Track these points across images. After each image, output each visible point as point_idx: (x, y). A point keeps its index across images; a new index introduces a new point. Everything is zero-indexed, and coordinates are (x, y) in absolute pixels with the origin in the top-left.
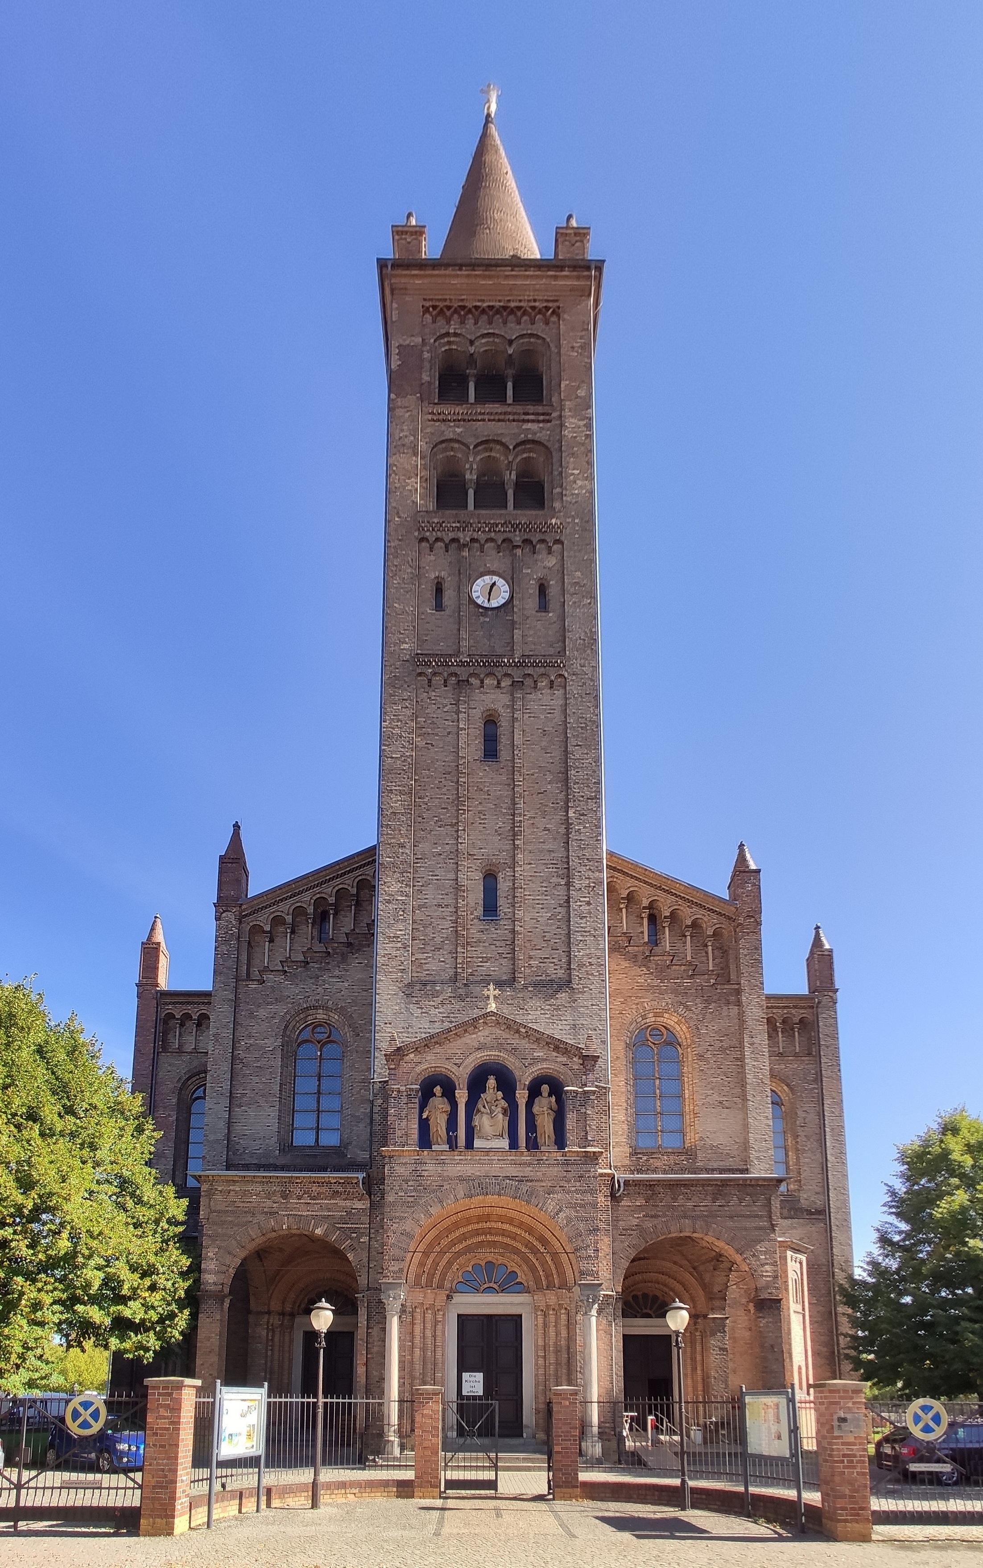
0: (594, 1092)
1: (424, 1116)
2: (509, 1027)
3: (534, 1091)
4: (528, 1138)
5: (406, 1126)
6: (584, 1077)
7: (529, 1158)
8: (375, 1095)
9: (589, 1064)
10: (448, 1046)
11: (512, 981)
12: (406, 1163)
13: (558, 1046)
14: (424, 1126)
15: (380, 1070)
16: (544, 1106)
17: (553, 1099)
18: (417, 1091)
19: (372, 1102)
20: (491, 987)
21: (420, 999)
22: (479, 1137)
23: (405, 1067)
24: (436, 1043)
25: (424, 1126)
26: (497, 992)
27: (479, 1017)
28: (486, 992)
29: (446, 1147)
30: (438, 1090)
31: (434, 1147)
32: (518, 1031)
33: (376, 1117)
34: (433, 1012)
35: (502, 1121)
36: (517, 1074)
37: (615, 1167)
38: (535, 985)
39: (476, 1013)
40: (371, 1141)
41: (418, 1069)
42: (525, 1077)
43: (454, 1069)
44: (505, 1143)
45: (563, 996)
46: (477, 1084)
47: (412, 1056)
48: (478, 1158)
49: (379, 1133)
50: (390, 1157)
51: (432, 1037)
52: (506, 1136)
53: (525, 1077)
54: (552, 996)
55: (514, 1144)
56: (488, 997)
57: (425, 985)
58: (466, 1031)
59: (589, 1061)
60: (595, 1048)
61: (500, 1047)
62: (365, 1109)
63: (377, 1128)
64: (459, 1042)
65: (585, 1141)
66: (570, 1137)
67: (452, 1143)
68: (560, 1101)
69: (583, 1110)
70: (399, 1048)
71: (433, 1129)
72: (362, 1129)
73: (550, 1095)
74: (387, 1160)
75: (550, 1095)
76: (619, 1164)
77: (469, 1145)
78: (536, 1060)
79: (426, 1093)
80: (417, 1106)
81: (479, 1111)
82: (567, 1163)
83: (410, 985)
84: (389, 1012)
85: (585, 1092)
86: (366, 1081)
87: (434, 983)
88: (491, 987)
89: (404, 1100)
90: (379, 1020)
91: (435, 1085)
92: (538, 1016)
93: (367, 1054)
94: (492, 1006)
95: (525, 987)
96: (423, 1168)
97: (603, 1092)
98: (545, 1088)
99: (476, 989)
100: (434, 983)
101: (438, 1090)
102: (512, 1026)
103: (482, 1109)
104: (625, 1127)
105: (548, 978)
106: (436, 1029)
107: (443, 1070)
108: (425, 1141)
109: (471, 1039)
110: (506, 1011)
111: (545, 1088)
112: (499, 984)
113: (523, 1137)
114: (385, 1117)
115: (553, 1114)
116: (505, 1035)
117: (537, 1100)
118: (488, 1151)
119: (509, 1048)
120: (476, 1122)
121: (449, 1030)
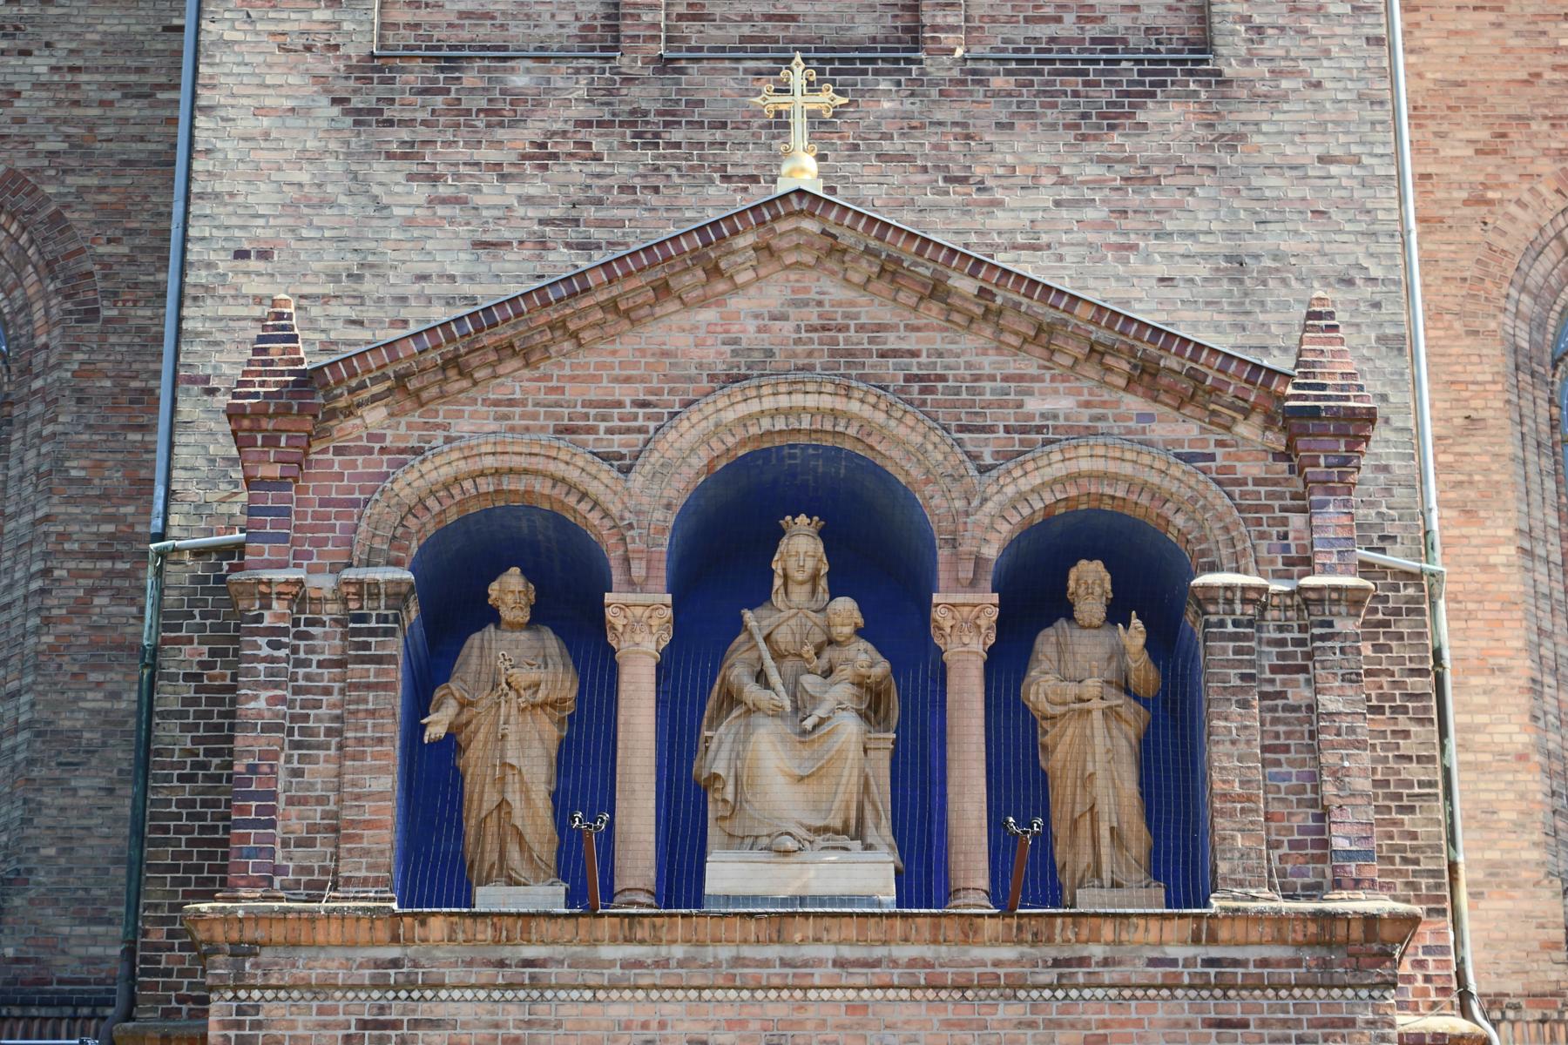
0: (1353, 600)
1: (437, 726)
2: (891, 271)
3: (1031, 595)
4: (1000, 846)
5: (333, 783)
6: (1297, 520)
7: (1008, 953)
8: (169, 620)
9: (1322, 452)
10: (564, 364)
11: (907, 43)
12: (323, 987)
13: (1153, 364)
14: (433, 779)
15: (202, 482)
16: (1085, 671)
17: (1135, 635)
18: (398, 596)
19: (152, 659)
20: (798, 75)
21: (423, 133)
22: (734, 840)
23: (335, 471)
24: (507, 350)
25: (433, 779)
26: (826, 99)
27: (729, 225)
28: (767, 101)
29: (550, 895)
30: (510, 590)
31: (488, 897)
32: (937, 291)
33: (173, 737)
34: (492, 194)
35: (855, 751)
36: (938, 503)
37: (1494, 1001)
38: (1025, 62)
39: (718, 200)
40: (137, 869)
41: (408, 483)
42: (977, 521)
43: (601, 483)
44: (872, 873)
45: (1171, 120)
46: (722, 556)
47: (375, 416)
48: (725, 952)
49: (188, 822)
50: (241, 951)
51: (484, 319)
52: (881, 831)
53: (977, 521)
54: (1112, 118)
55: (924, 880)
56: (781, 123)
57: (451, 62)
58: (663, 290)
59: (1319, 433)
60: (1352, 366)
61: (845, 368)
62: (103, 698)
63: (171, 793)
64: (630, 344)
65: (1315, 856)
66: (1236, 840)
67: (585, 873)
68: (1168, 642)
69: (1299, 693)
70: (307, 381)
71: (481, 797)
72: (90, 805)
73: (1116, 614)
74: (221, 967)
75: (1116, 614)
76: (1513, 986)
77: (680, 881)
78: (1036, 435)
79: (448, 608)
80: (396, 674)
81: (731, 699)
82: (1219, 978)
83: (376, 66)
84: (263, 197)
85: (1307, 600)
86: (125, 551)
87: (502, 55)
88: (798, 75)
89: (327, 642)
90: (208, 240)
91: (500, 567)
92: (1033, 205)
93: (137, 406)
94: (802, 169)
95: (973, 74)
96: (422, 1011)
97: (1400, 601)
98: (1090, 581)
99: (719, 87)
100: (502, 55)
101: (510, 590)
102: (906, 266)
103: (752, 692)
104: (1534, 783)
105: (1093, 31)
106: (507, 277)
107: (541, 486)
108: (436, 860)
109: (688, 333)
110: (874, 190)
111: (1090, 581)
112: (838, 61)
113: (977, 844)
114: (219, 725)
115: (1134, 718)
116: (873, 309)
117: (1046, 643)
118: (782, 917)
119: (892, 371)
120: (719, 753)
121: (576, 285)
